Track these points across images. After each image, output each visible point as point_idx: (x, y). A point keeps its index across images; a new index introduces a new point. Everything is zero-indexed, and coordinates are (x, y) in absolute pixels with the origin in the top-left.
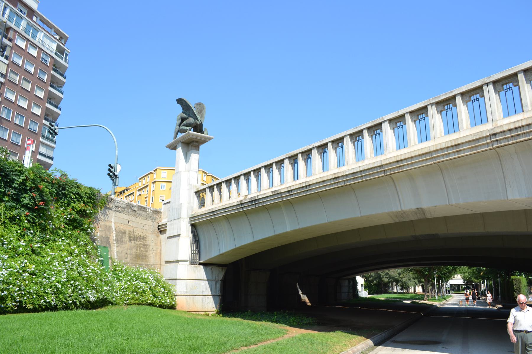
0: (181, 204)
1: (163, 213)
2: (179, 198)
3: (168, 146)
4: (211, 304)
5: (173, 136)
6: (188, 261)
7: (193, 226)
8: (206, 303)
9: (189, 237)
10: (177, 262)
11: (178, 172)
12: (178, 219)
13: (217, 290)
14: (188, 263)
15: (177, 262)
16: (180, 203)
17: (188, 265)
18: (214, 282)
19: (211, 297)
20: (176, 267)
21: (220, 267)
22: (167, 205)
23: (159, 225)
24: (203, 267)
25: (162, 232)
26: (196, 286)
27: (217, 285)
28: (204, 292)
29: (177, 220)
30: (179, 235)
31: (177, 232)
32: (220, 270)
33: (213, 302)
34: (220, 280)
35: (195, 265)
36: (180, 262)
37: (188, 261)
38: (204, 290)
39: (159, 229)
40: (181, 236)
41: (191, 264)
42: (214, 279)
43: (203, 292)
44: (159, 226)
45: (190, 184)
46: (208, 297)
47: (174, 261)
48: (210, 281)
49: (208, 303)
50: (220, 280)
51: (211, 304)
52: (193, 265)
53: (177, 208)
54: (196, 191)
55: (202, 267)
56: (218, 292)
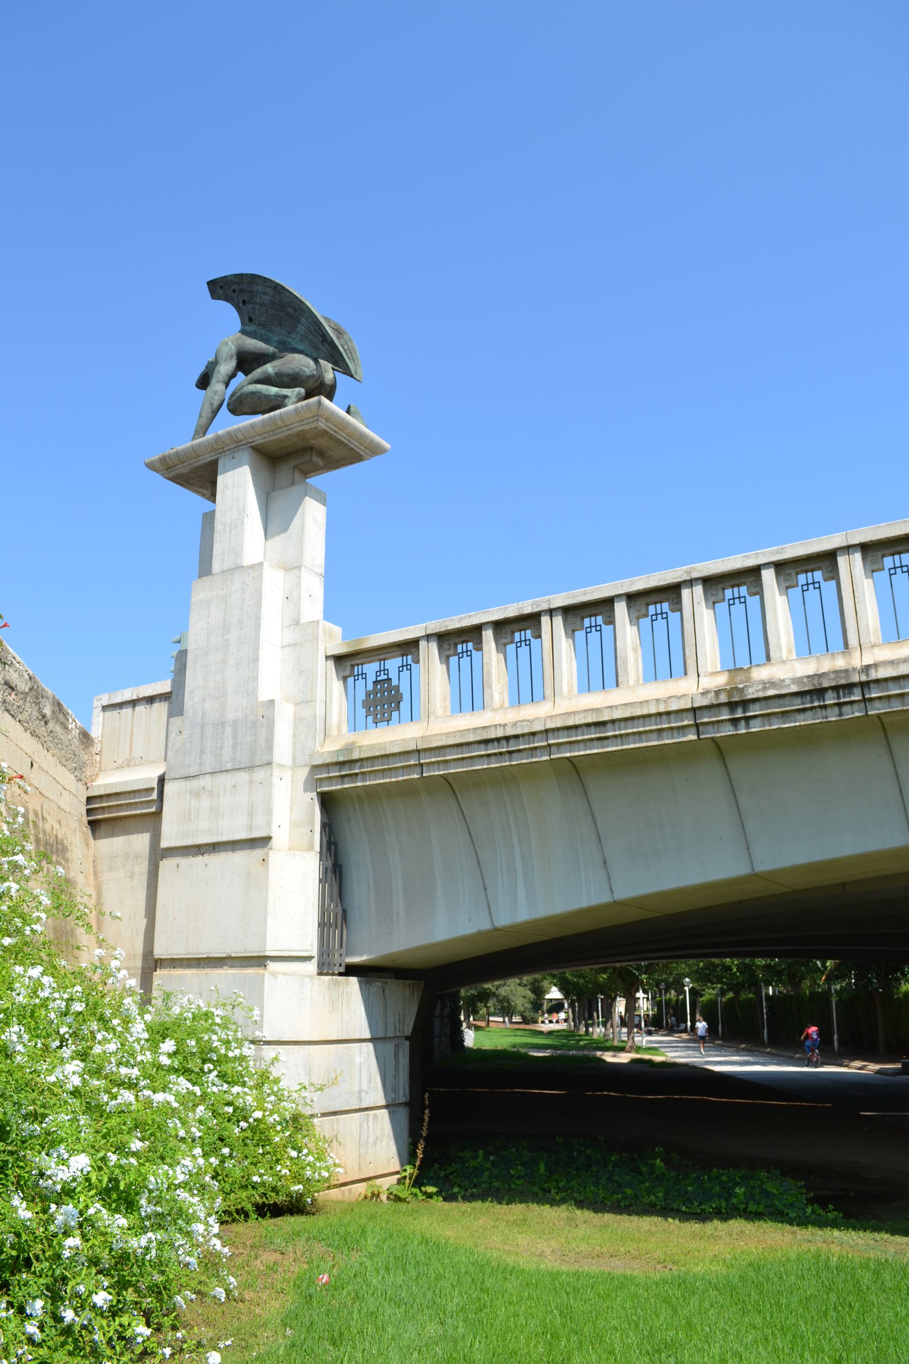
0: (272, 702)
1: (97, 748)
2: (256, 679)
3: (163, 460)
4: (384, 1144)
5: (192, 424)
6: (309, 958)
7: (327, 802)
8: (371, 1140)
9: (311, 848)
10: (260, 961)
11: (240, 568)
12: (251, 768)
13: (401, 1080)
14: (311, 967)
15: (260, 961)
16: (263, 696)
17: (311, 977)
18: (390, 1047)
19: (385, 1112)
20: (258, 987)
21: (408, 982)
22: (115, 713)
23: (91, 793)
24: (360, 983)
25: (103, 828)
26: (338, 1072)
27: (401, 1060)
28: (363, 1094)
29: (243, 776)
30: (265, 841)
31: (250, 827)
32: (407, 992)
33: (391, 1134)
34: (407, 1038)
35: (333, 974)
36: (272, 966)
37: (309, 958)
38: (365, 1087)
39: (89, 812)
40: (274, 843)
41: (320, 974)
42: (390, 1034)
43: (360, 1092)
44: (89, 800)
45: (304, 619)
46: (375, 1116)
47: (229, 958)
48: (379, 1045)
49: (375, 1143)
50: (407, 1038)
51: (384, 1144)
52: (327, 974)
53: (235, 723)
54: (341, 649)
55: (354, 980)
56: (403, 1095)
